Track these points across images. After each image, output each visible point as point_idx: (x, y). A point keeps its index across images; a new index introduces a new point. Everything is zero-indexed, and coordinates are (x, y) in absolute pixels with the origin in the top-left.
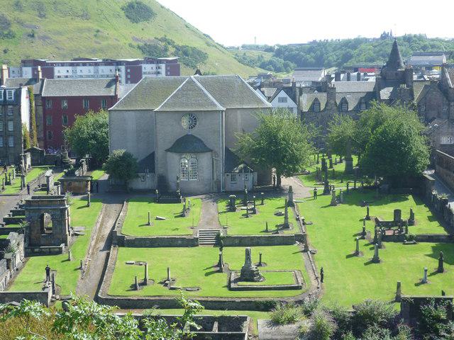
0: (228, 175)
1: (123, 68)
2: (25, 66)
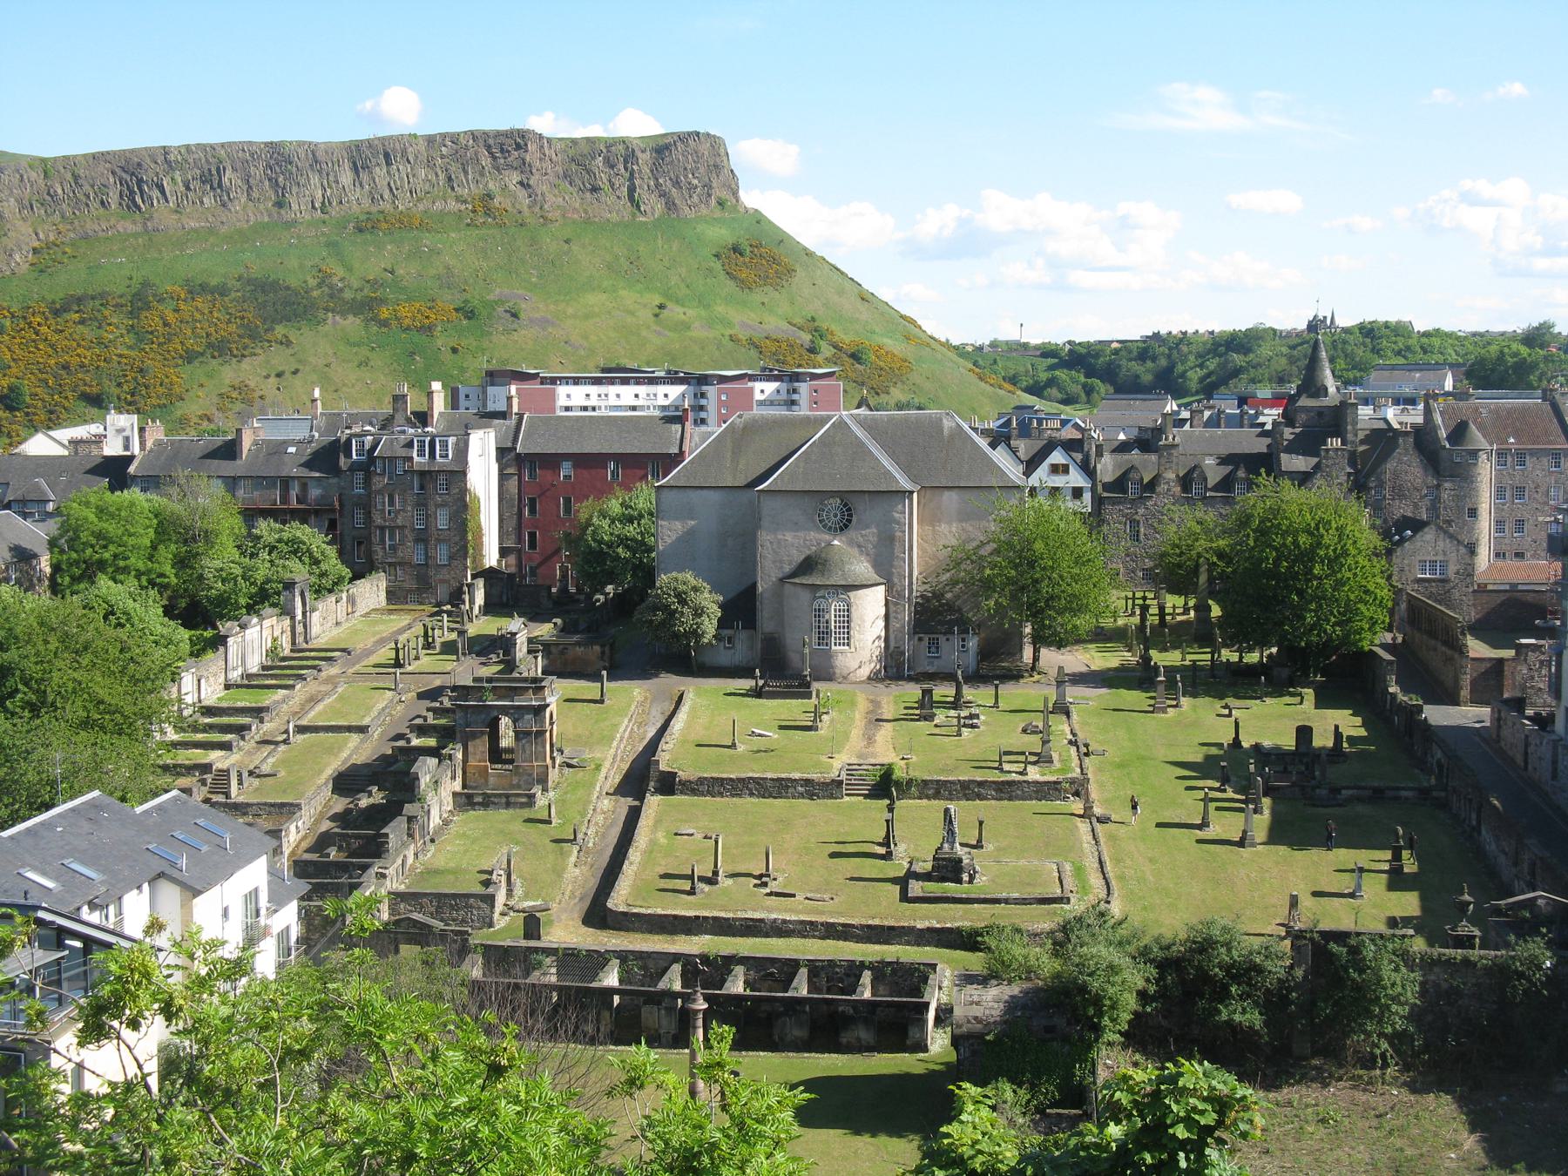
0: (920, 639)
1: (711, 391)
2: (492, 385)
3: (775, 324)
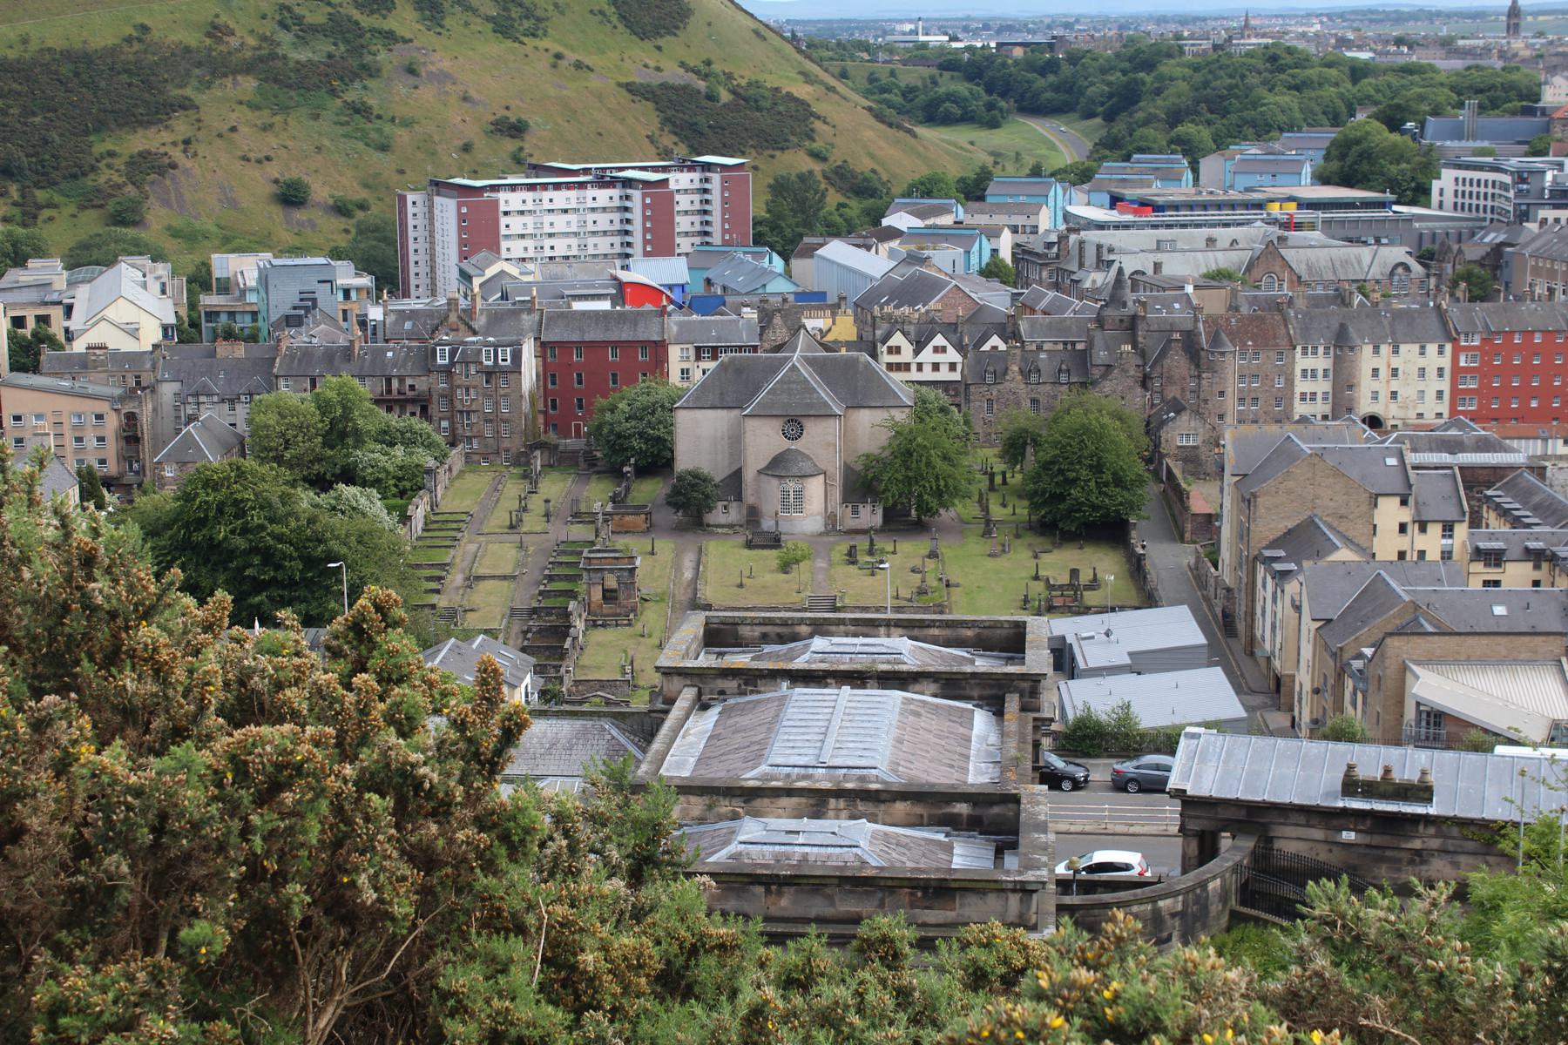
1: (636, 194)
3: (673, 74)
